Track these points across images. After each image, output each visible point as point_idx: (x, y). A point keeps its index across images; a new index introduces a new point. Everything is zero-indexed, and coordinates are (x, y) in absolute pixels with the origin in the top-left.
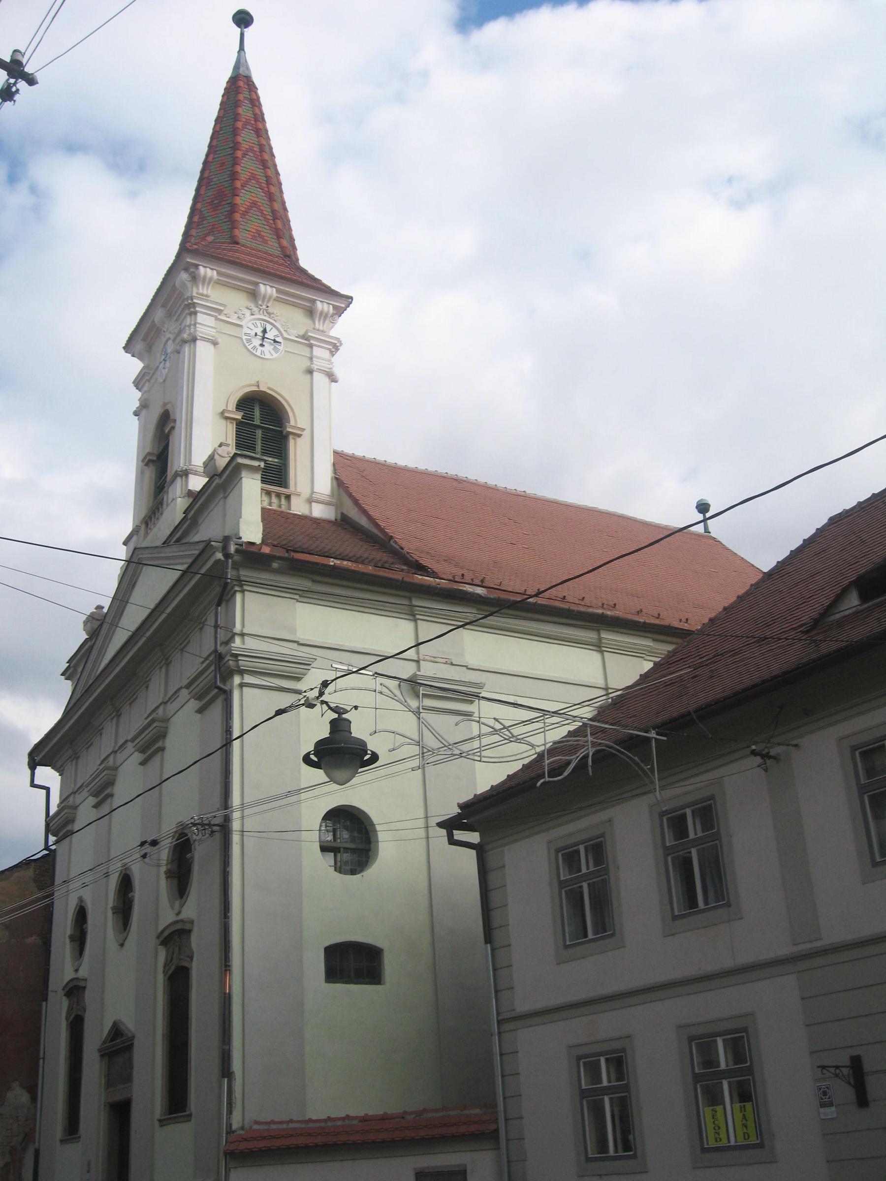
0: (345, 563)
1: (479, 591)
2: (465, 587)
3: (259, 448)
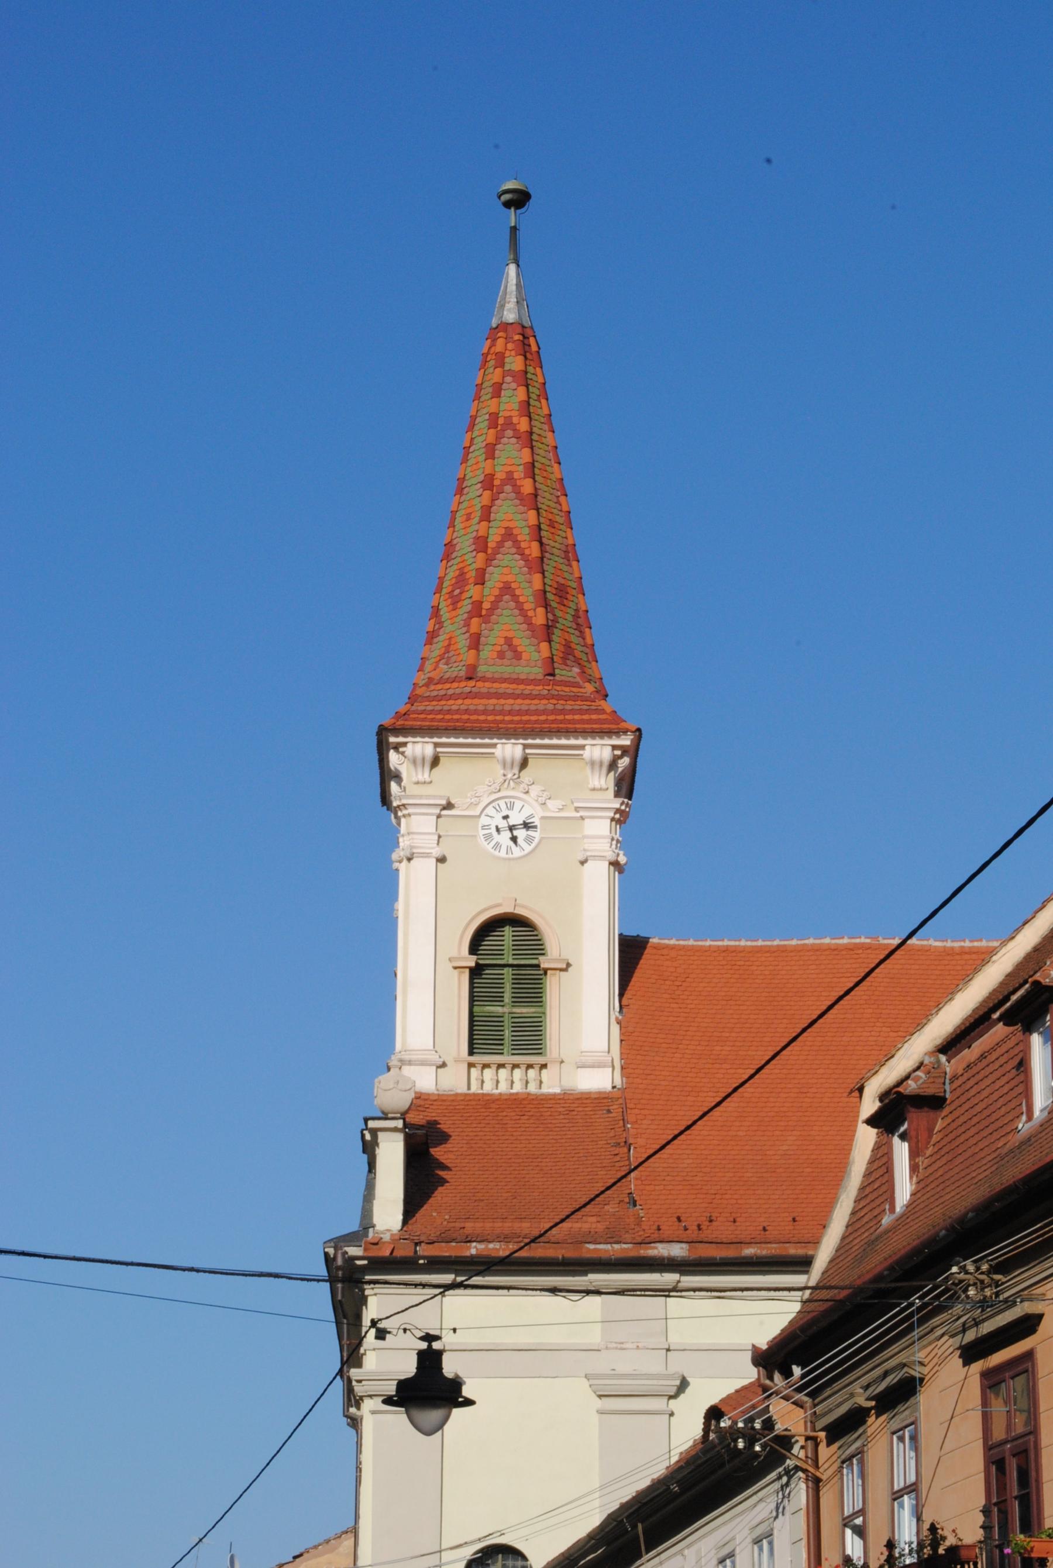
0: (491, 1246)
1: (677, 1251)
2: (656, 1248)
3: (507, 997)
